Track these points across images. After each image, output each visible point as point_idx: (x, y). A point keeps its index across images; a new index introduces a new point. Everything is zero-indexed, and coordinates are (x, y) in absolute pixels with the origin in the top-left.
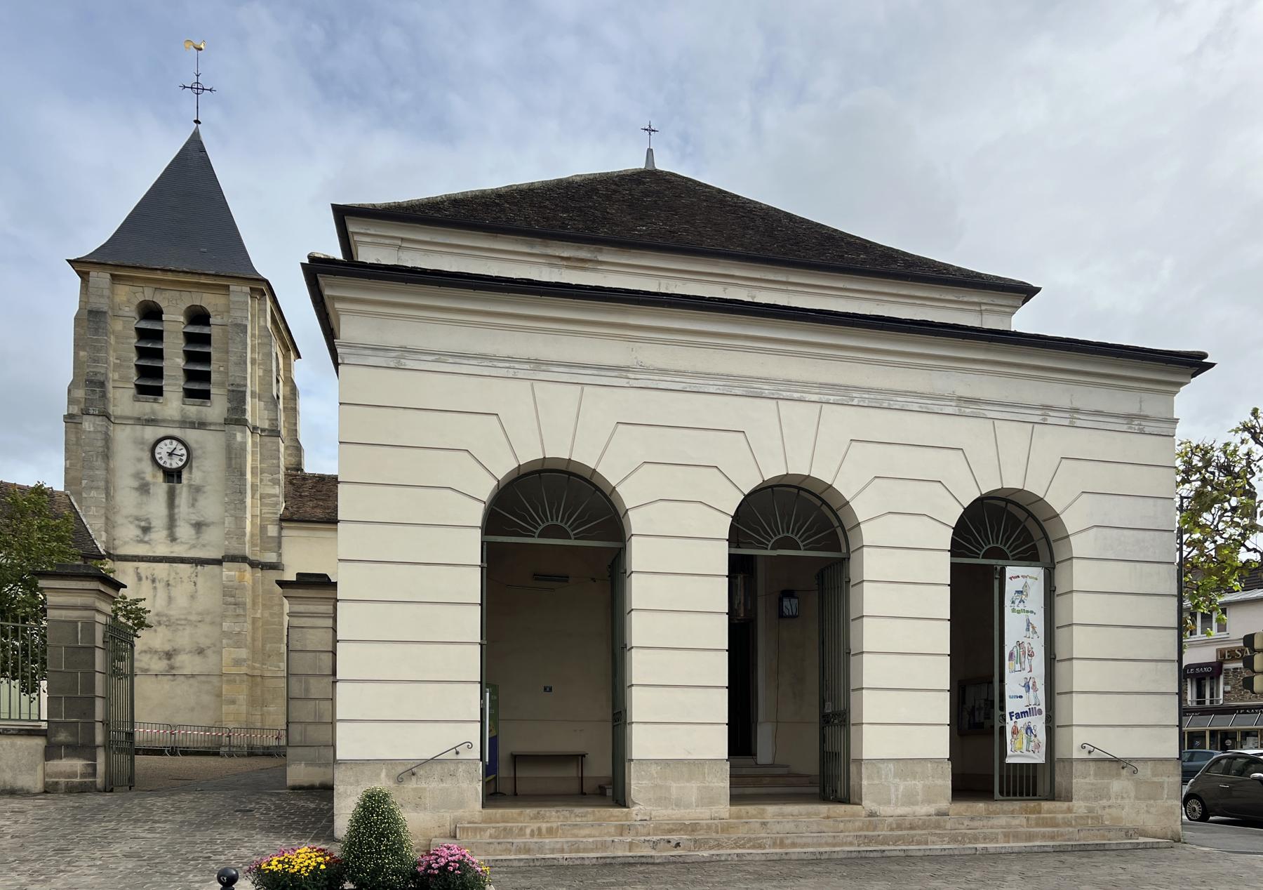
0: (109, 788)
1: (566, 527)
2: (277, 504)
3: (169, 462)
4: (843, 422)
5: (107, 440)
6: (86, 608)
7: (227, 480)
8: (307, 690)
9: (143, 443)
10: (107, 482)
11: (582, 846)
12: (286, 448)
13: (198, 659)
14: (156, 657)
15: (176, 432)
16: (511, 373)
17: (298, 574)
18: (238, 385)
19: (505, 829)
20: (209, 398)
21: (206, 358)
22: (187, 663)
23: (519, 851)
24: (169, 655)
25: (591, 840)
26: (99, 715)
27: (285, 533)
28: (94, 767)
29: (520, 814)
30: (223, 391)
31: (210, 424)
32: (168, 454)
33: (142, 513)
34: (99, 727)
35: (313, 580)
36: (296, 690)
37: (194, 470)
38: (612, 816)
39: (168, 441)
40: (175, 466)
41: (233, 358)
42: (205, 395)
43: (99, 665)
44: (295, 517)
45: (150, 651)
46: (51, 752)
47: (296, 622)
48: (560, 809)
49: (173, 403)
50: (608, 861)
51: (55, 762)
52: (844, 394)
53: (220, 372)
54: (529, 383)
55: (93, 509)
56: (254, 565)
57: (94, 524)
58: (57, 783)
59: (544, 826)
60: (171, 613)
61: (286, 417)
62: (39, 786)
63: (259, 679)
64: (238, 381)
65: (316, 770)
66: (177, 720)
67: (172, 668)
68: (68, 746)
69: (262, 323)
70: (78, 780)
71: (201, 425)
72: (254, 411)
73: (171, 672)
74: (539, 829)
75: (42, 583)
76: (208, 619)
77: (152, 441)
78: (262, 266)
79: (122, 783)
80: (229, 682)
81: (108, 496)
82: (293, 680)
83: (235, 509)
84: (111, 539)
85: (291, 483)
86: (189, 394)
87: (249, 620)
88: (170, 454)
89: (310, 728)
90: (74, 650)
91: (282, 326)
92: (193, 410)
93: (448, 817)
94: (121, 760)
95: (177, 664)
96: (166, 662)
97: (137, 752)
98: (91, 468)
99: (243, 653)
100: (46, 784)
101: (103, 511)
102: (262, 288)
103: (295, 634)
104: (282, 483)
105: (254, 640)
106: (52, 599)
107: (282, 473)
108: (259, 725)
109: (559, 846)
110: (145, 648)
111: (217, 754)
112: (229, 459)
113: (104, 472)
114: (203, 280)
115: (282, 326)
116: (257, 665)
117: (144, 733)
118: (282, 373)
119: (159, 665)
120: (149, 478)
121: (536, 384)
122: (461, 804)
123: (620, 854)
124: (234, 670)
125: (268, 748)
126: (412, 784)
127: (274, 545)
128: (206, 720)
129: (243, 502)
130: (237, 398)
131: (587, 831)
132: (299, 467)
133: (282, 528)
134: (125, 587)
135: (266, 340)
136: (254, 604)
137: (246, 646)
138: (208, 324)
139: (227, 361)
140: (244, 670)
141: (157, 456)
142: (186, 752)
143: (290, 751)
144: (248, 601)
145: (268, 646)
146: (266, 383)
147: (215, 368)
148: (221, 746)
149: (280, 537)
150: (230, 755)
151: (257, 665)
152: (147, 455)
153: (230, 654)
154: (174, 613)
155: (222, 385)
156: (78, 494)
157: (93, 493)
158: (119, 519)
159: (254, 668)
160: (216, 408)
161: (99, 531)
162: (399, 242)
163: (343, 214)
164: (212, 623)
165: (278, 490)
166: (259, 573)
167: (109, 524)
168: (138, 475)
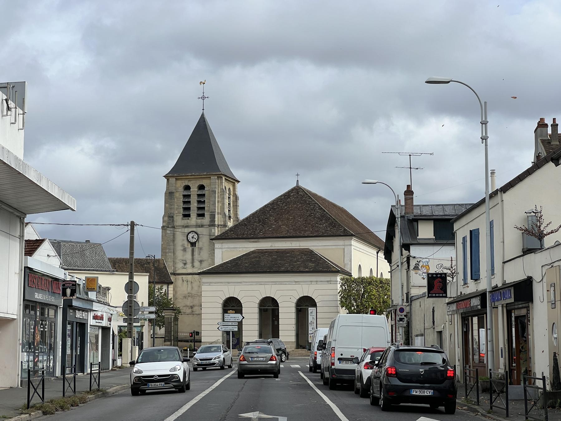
15: (194, 229)
30: (209, 213)
33: (184, 258)
41: (211, 203)
49: (194, 219)
71: (202, 226)
81: (174, 253)
88: (193, 237)
92: (200, 221)
94: (176, 343)
97: (180, 341)
120: (186, 246)
130: (213, 217)
147: (206, 205)
152: (186, 238)
160: (206, 220)
167: (174, 263)
168: (183, 245)
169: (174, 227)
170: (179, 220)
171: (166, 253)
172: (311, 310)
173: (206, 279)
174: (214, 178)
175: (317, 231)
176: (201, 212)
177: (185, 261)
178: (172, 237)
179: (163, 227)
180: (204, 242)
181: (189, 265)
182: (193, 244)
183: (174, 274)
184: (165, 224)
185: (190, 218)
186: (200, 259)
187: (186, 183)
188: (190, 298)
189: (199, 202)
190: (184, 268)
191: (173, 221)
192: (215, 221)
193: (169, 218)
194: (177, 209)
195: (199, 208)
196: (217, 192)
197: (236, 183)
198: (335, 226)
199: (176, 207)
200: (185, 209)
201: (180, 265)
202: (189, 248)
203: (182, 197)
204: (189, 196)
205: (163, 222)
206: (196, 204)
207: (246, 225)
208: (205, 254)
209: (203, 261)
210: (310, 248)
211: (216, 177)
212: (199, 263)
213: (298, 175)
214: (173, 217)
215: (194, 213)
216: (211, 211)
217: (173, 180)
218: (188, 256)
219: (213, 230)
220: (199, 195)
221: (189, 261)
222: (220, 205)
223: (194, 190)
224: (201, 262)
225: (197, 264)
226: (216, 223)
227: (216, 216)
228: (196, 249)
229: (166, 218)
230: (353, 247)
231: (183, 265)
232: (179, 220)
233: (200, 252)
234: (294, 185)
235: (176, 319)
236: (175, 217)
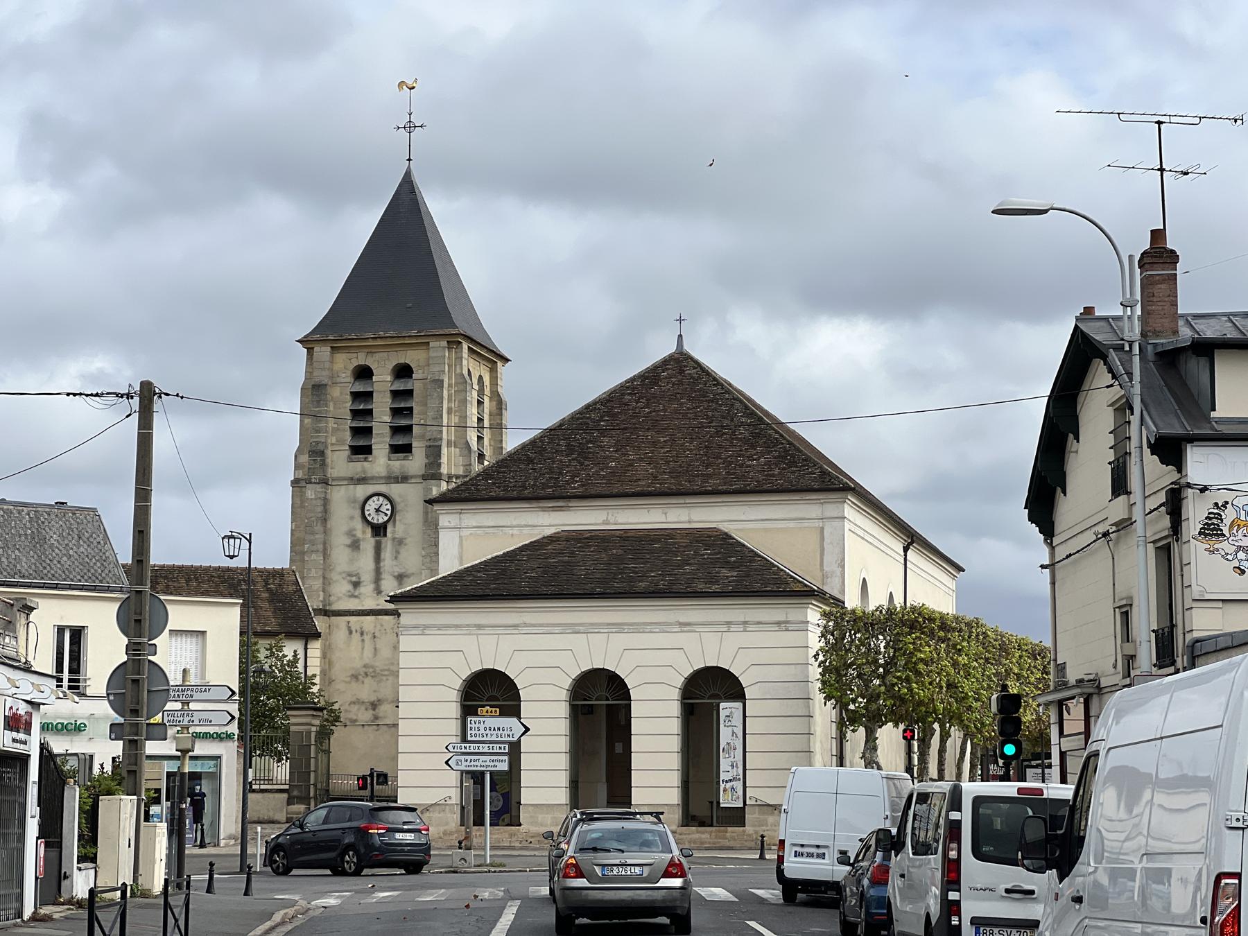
4: (620, 640)
9: (355, 501)
15: (383, 488)
18: (435, 440)
31: (412, 477)
32: (377, 510)
33: (352, 569)
39: (375, 498)
40: (381, 521)
41: (431, 414)
49: (380, 461)
52: (620, 627)
64: (436, 435)
69: (458, 371)
71: (404, 479)
77: (362, 499)
84: (328, 595)
88: (377, 510)
92: (397, 465)
101: (320, 573)
120: (359, 534)
130: (434, 453)
135: (461, 387)
139: (425, 413)
152: (358, 513)
155: (422, 436)
158: (334, 576)
160: (416, 462)
161: (317, 591)
167: (326, 581)
168: (350, 533)
169: (325, 482)
170: (339, 462)
171: (303, 553)
172: (728, 708)
173: (411, 616)
174: (438, 345)
175: (742, 478)
176: (401, 441)
177: (357, 575)
178: (320, 509)
179: (295, 483)
180: (409, 523)
181: (367, 588)
182: (379, 530)
183: (326, 613)
184: (300, 475)
186: (397, 570)
187: (361, 359)
188: (368, 680)
189: (396, 412)
190: (353, 596)
191: (324, 464)
192: (439, 465)
194: (335, 430)
195: (396, 430)
196: (446, 385)
197: (499, 364)
198: (792, 464)
200: (356, 432)
201: (341, 588)
202: (368, 541)
203: (349, 397)
204: (368, 396)
206: (387, 419)
207: (530, 460)
208: (411, 558)
209: (408, 576)
210: (725, 527)
211: (444, 343)
213: (680, 320)
214: (322, 453)
215: (381, 442)
216: (428, 436)
217: (323, 352)
218: (366, 563)
220: (396, 394)
221: (367, 577)
223: (383, 380)
226: (444, 470)
227: (444, 451)
228: (387, 544)
229: (305, 458)
230: (847, 525)
231: (350, 587)
232: (339, 462)
233: (398, 552)
234: (672, 349)
235: (324, 734)
236: (328, 452)
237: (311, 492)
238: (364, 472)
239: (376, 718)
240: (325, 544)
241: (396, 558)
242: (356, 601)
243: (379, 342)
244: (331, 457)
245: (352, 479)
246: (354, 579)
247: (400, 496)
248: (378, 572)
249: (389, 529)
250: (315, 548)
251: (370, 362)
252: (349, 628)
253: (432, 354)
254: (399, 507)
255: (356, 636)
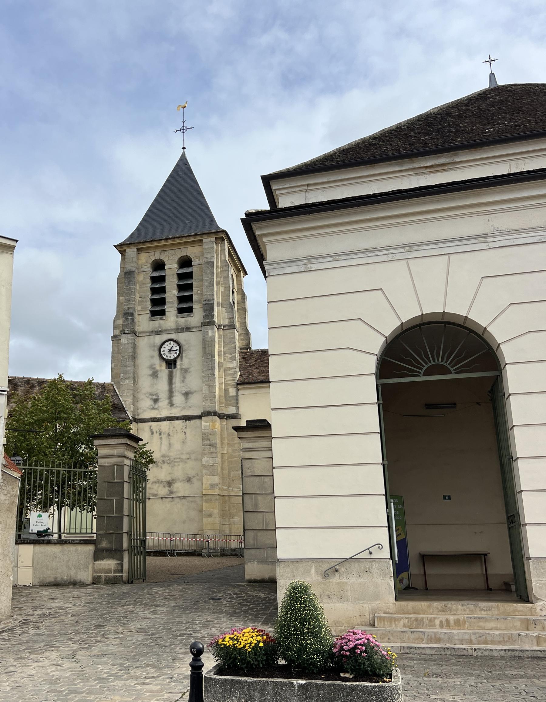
0: (130, 581)
1: (447, 365)
2: (235, 373)
3: (169, 355)
5: (134, 347)
6: (119, 456)
7: (203, 362)
8: (256, 505)
9: (154, 346)
10: (134, 373)
11: (489, 638)
12: (240, 335)
13: (187, 485)
14: (162, 485)
15: (173, 336)
16: (390, 257)
17: (247, 421)
18: (209, 300)
19: (416, 620)
20: (192, 311)
21: (189, 287)
22: (181, 489)
23: (430, 640)
24: (169, 484)
25: (497, 632)
26: (125, 529)
27: (240, 392)
28: (122, 565)
29: (429, 606)
30: (200, 306)
31: (193, 328)
34: (125, 537)
35: (258, 424)
36: (249, 507)
37: (184, 358)
38: (516, 610)
39: (168, 343)
40: (172, 358)
41: (206, 284)
42: (189, 310)
43: (126, 495)
44: (247, 381)
45: (159, 482)
46: (97, 556)
47: (247, 455)
48: (465, 603)
50: (517, 654)
51: (99, 562)
53: (198, 294)
54: (404, 261)
55: (126, 391)
56: (221, 416)
57: (126, 400)
58: (100, 577)
59: (452, 618)
60: (171, 454)
61: (239, 315)
62: (89, 580)
63: (227, 498)
64: (209, 297)
65: (266, 566)
66: (175, 530)
67: (171, 492)
68: (107, 550)
69: (223, 258)
70: (112, 575)
71: (188, 329)
72: (219, 315)
73: (171, 496)
74: (447, 621)
75: (96, 442)
76: (193, 457)
78: (222, 224)
79: (138, 577)
80: (207, 501)
82: (247, 497)
83: (209, 380)
84: (136, 409)
85: (243, 358)
86: (181, 311)
87: (219, 455)
88: (170, 351)
89: (259, 534)
90: (112, 484)
91: (235, 257)
92: (183, 321)
93: (367, 607)
95: (175, 490)
96: (168, 488)
97: (149, 554)
98: (126, 366)
99: (216, 479)
100: (94, 578)
101: (131, 392)
102: (222, 236)
103: (246, 464)
104: (238, 359)
105: (222, 469)
106: (101, 452)
107: (237, 352)
108: (227, 532)
109: (466, 637)
110: (155, 480)
111: (200, 555)
112: (204, 348)
113: (133, 368)
114: (188, 240)
115: (235, 257)
116: (225, 488)
117: (153, 540)
118: (236, 287)
119: (163, 491)
120: (157, 367)
121: (411, 262)
122: (376, 597)
123: (528, 647)
124: (210, 492)
125: (234, 550)
126: (335, 579)
127: (234, 401)
128: (193, 529)
129: (213, 375)
130: (209, 308)
131: (492, 625)
132: (248, 347)
133: (238, 390)
134: (142, 440)
135: (225, 268)
136: (222, 443)
137: (218, 474)
138: (190, 266)
139: (202, 286)
140: (217, 491)
141: (162, 353)
142: (180, 554)
143: (246, 552)
144: (218, 442)
145: (232, 473)
146: (226, 296)
147: (195, 293)
148: (202, 549)
149: (237, 395)
150: (209, 556)
151: (225, 488)
152: (157, 353)
153: (207, 480)
154: (173, 454)
155: (200, 301)
156: (118, 383)
157: (127, 382)
158: (141, 396)
159: (223, 490)
161: (129, 405)
162: (306, 188)
163: (267, 180)
164: (196, 459)
165: (235, 365)
166: (224, 422)
168: (152, 367)
170: (144, 322)
177: (157, 394)
179: (115, 338)
181: (164, 403)
182: (171, 364)
184: (117, 332)
185: (164, 317)
186: (184, 390)
188: (165, 466)
189: (181, 288)
190: (153, 408)
191: (133, 321)
192: (213, 316)
193: (126, 316)
195: (181, 299)
199: (138, 298)
200: (154, 302)
201: (145, 403)
202: (164, 371)
203: (149, 280)
204: (162, 279)
205: (115, 328)
206: (175, 292)
208: (194, 381)
212: (183, 398)
214: (132, 314)
217: (131, 252)
218: (162, 386)
219: (210, 333)
220: (181, 277)
222: (222, 289)
223: (172, 269)
224: (187, 395)
225: (178, 399)
226: (216, 319)
227: (215, 307)
228: (177, 373)
231: (152, 403)
232: (144, 322)
237: (124, 340)
238: (160, 326)
239: (171, 492)
240: (134, 373)
241: (183, 381)
242: (156, 411)
243: (169, 242)
244: (137, 318)
245: (152, 332)
246: (154, 397)
247: (185, 340)
248: (171, 391)
249: (178, 363)
250: (127, 376)
251: (164, 257)
252: (151, 430)
253: (205, 246)
254: (184, 348)
255: (156, 436)
